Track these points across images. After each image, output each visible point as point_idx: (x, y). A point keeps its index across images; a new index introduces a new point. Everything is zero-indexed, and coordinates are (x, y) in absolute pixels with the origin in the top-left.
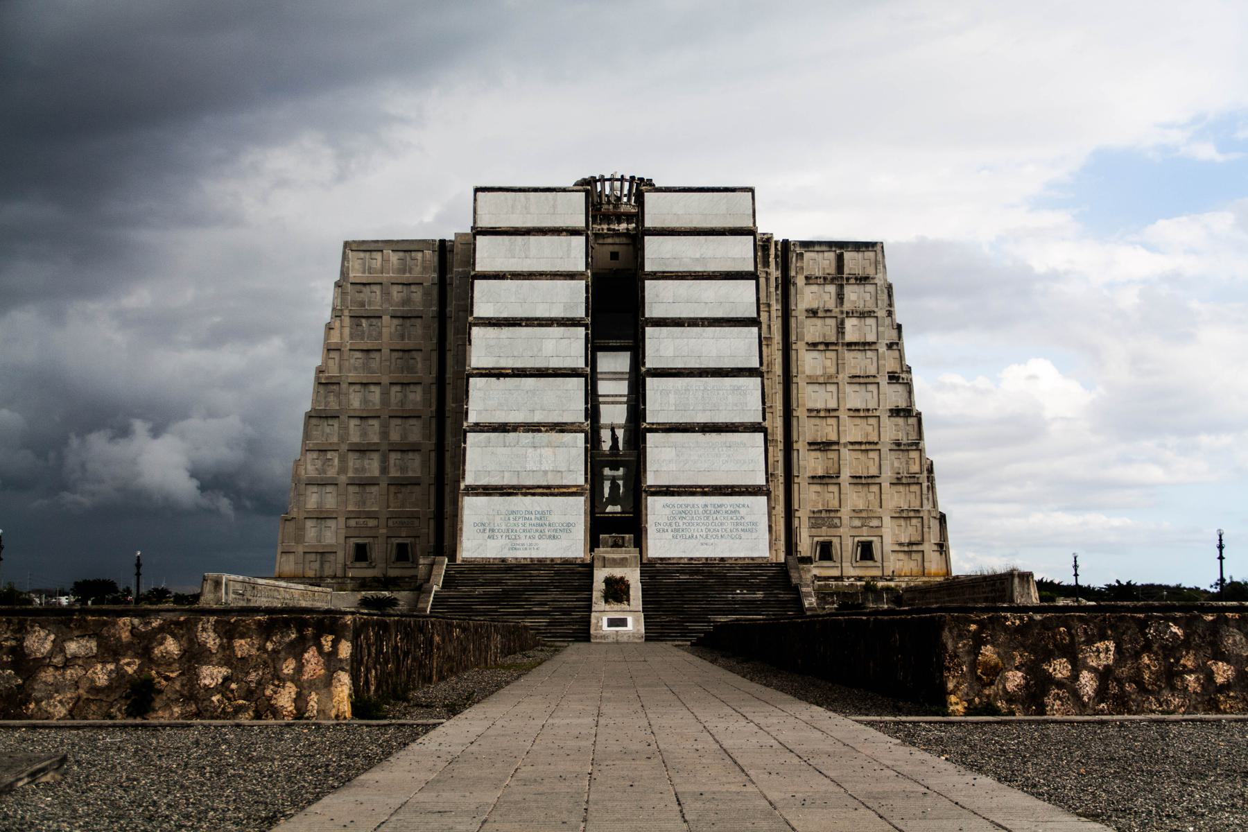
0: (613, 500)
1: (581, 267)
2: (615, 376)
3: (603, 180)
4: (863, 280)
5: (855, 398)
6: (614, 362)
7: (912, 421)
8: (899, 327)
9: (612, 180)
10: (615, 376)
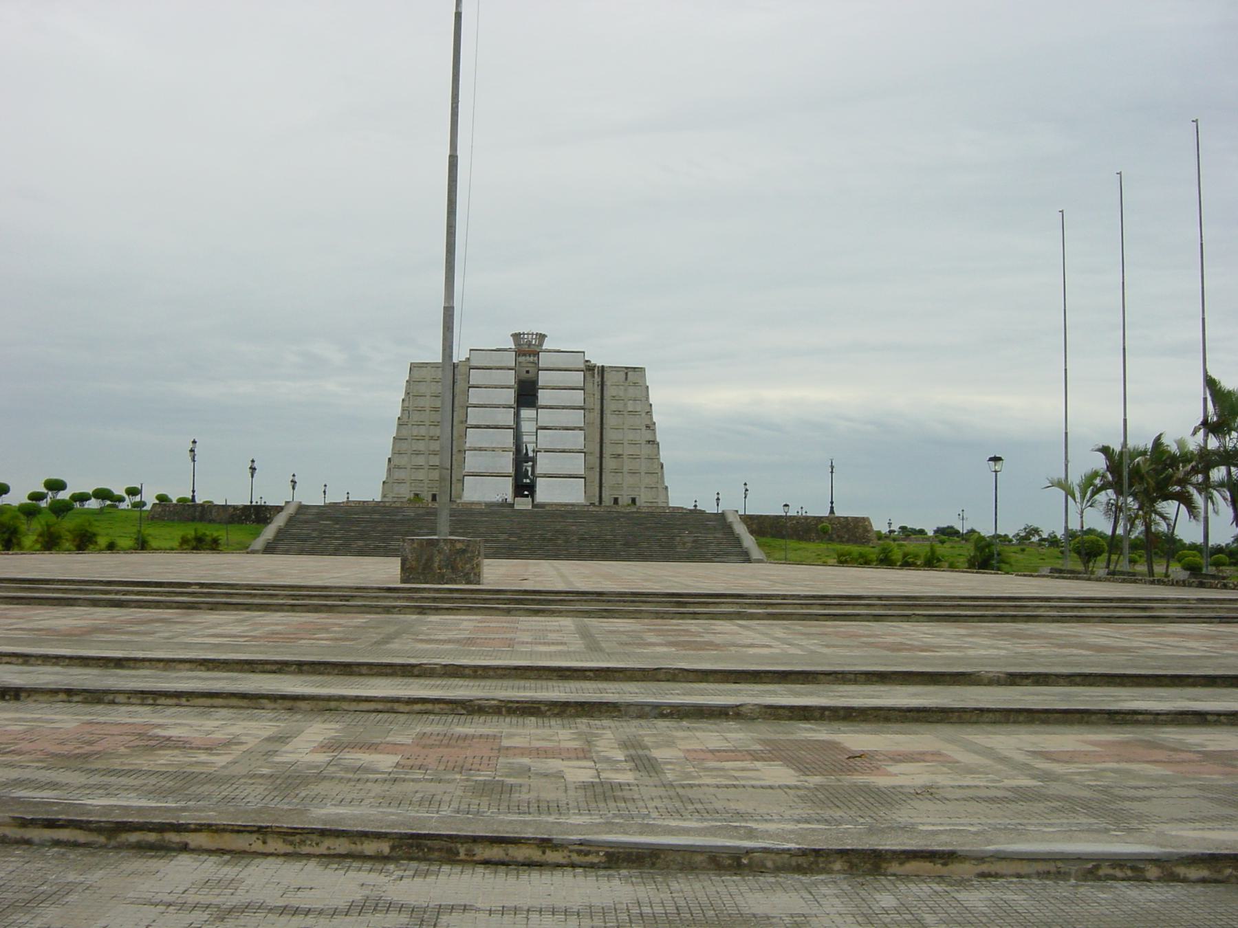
0: (527, 477)
1: (512, 382)
2: (530, 420)
3: (524, 334)
4: (635, 384)
5: (631, 436)
6: (526, 413)
7: (655, 446)
8: (651, 405)
9: (528, 334)
10: (530, 420)
